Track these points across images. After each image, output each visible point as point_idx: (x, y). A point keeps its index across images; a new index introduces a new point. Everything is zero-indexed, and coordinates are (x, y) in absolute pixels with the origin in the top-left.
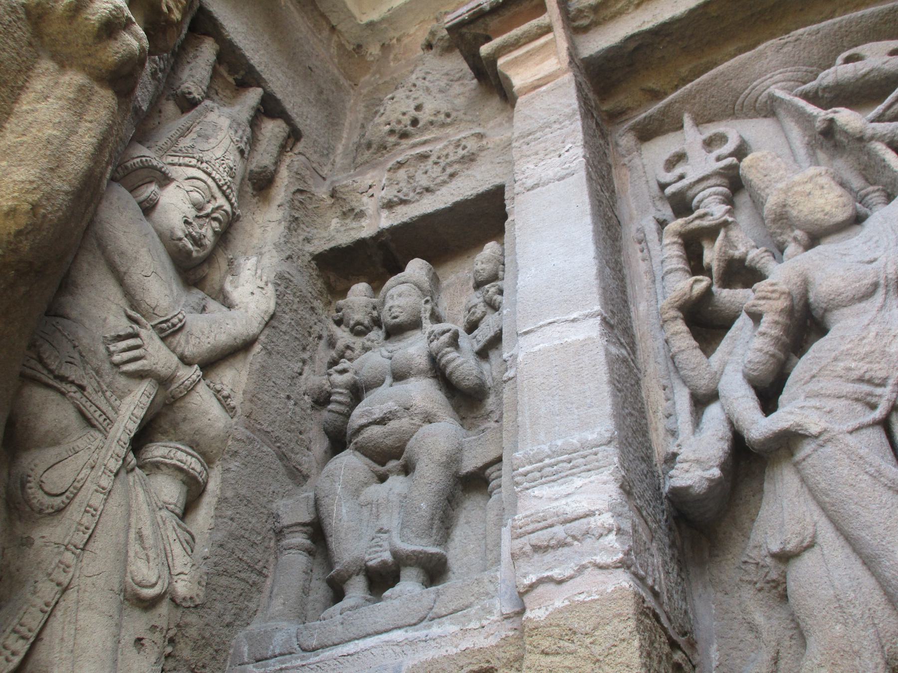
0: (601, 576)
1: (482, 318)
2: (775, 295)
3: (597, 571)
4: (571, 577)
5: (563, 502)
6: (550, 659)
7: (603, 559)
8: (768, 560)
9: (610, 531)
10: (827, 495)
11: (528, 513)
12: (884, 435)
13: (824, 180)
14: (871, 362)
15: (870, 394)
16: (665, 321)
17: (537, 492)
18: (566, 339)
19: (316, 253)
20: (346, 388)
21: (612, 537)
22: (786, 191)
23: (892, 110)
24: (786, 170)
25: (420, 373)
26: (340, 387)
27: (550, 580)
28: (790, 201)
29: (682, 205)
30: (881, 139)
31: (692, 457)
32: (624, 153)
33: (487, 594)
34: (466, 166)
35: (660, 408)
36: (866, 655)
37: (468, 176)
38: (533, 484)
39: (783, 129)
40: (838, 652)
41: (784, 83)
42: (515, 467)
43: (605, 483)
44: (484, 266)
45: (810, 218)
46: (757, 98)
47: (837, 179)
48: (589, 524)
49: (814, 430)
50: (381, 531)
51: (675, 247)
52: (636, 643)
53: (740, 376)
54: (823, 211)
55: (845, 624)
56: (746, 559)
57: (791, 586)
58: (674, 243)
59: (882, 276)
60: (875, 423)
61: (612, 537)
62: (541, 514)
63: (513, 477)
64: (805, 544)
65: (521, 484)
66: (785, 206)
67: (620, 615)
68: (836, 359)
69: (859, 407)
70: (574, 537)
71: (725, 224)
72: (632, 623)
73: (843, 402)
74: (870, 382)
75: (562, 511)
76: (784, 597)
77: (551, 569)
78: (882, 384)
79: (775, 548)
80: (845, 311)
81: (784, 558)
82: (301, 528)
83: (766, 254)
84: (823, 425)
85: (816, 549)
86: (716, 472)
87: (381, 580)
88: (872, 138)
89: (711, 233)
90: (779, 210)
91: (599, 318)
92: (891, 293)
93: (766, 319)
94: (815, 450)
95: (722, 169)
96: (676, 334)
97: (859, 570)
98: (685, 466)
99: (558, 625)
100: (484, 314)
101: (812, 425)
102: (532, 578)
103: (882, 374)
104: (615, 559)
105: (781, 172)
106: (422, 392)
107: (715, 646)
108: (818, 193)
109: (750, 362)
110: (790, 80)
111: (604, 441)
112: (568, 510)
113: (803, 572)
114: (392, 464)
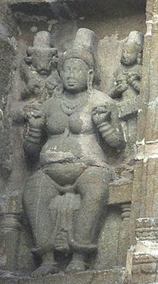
1: (125, 90)
19: (12, 3)
20: (39, 128)
25: (87, 132)
26: (35, 128)
38: (144, 238)
50: (62, 230)
62: (147, 255)
82: (14, 216)
87: (63, 257)
100: (126, 89)
106: (87, 145)
114: (69, 187)
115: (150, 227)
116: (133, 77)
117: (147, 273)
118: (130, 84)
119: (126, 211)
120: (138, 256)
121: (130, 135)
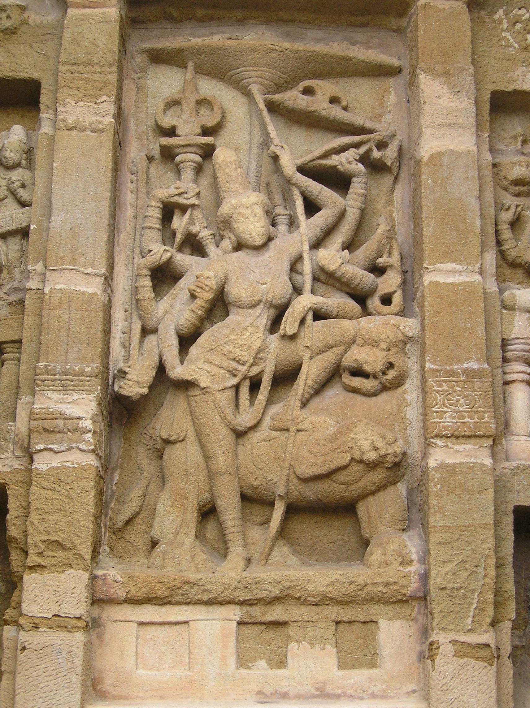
0: (80, 455)
2: (207, 289)
3: (79, 452)
4: (63, 451)
5: (65, 406)
6: (46, 492)
7: (83, 446)
8: (158, 439)
9: (89, 431)
10: (198, 420)
11: (43, 406)
12: (234, 393)
13: (259, 210)
14: (242, 350)
15: (236, 370)
16: (139, 275)
17: (50, 394)
18: (80, 288)
21: (90, 435)
22: (235, 208)
23: (312, 163)
24: (240, 184)
27: (51, 450)
28: (235, 216)
29: (168, 155)
30: (299, 188)
31: (136, 379)
32: (136, 69)
33: (5, 439)
34: (7, 37)
35: (120, 324)
36: (191, 500)
37: (9, 51)
39: (251, 117)
40: (179, 495)
41: (263, 80)
42: (37, 373)
43: (90, 401)
44: (12, 155)
45: (242, 235)
46: (243, 79)
47: (266, 208)
48: (78, 424)
49: (203, 385)
51: (157, 210)
52: (93, 494)
53: (173, 327)
54: (250, 235)
55: (186, 483)
56: (146, 432)
57: (165, 456)
58: (158, 207)
59: (265, 297)
60: (233, 386)
61: (90, 435)
62: (51, 410)
63: (35, 380)
64: (179, 439)
65: (40, 386)
66: (231, 217)
67: (87, 478)
68: (226, 343)
69: (228, 375)
70: (69, 430)
71: (193, 206)
72: (92, 483)
73: (222, 371)
74: (238, 362)
75: (63, 412)
76: (161, 457)
77: (53, 444)
78: (243, 364)
79: (165, 437)
80: (241, 311)
81: (167, 442)
83: (210, 237)
84: (208, 384)
85: (184, 443)
86: (145, 391)
88: (294, 184)
89: (184, 209)
90: (227, 218)
91: (103, 278)
92: (266, 308)
93: (198, 302)
94: (200, 395)
95: (203, 144)
96: (145, 287)
97: (200, 459)
98: (131, 383)
99: (53, 476)
100: (6, 197)
101: (202, 382)
102: (40, 447)
103: (245, 359)
104: (90, 448)
105: (237, 186)
107: (117, 472)
108: (252, 219)
109: (181, 325)
110: (267, 79)
111: (94, 375)
112: (68, 412)
113: (174, 454)
115: (55, 375)
116: (18, 184)
117: (51, 432)
118: (13, 193)
119: (8, 353)
120: (39, 411)
121: (10, 257)
